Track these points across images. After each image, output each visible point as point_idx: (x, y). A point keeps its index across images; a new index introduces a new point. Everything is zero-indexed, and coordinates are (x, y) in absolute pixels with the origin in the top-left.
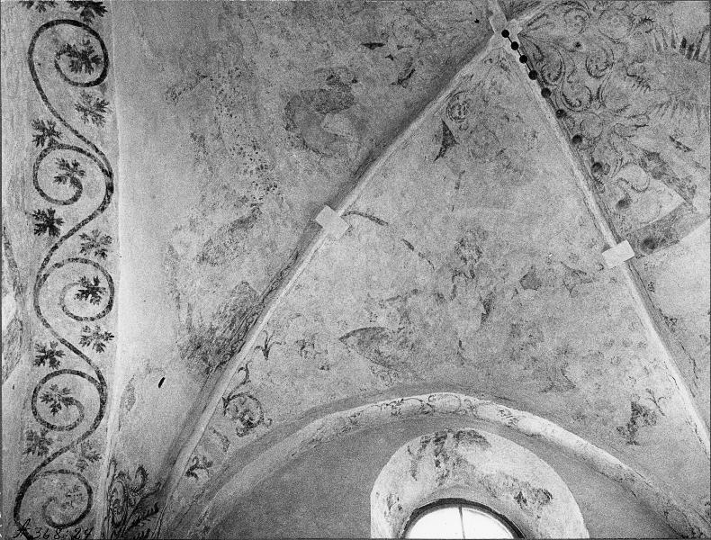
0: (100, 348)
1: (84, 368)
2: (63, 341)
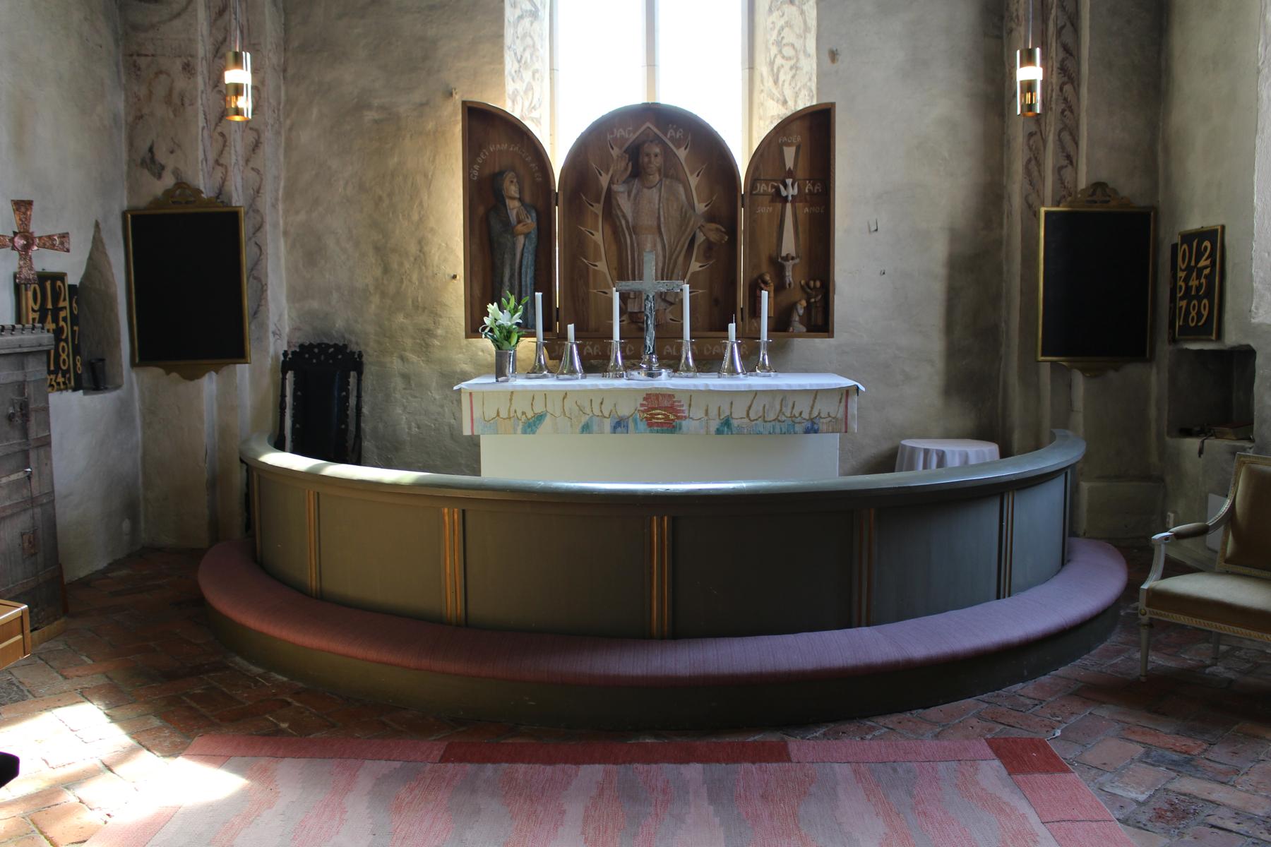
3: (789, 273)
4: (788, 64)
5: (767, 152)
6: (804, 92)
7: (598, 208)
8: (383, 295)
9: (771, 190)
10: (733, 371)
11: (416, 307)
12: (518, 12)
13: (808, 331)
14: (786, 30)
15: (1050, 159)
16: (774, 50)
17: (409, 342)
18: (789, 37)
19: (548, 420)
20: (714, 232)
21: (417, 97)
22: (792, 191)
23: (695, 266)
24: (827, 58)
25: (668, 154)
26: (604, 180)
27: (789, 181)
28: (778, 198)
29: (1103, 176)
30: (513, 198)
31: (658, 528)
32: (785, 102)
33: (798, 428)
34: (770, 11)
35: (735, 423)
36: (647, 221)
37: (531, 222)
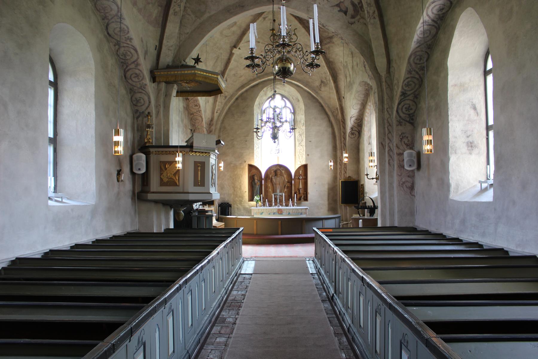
0: (200, 112)
1: (197, 115)
2: (194, 112)
3: (301, 191)
4: (301, 156)
5: (297, 171)
6: (303, 161)
7: (270, 181)
8: (234, 195)
9: (298, 178)
10: (290, 206)
11: (239, 196)
12: (256, 148)
13: (304, 200)
14: (301, 150)
15: (343, 172)
16: (299, 153)
17: (238, 203)
18: (301, 151)
19: (264, 213)
20: (288, 185)
21: (240, 162)
22: (301, 178)
23: (286, 190)
24: (307, 156)
25: (281, 172)
26: (271, 176)
27: (301, 176)
28: (299, 179)
29: (350, 175)
30: (256, 179)
31: (279, 222)
32: (301, 162)
33: (300, 214)
34: (298, 146)
35: (290, 213)
36: (278, 183)
37: (259, 183)
